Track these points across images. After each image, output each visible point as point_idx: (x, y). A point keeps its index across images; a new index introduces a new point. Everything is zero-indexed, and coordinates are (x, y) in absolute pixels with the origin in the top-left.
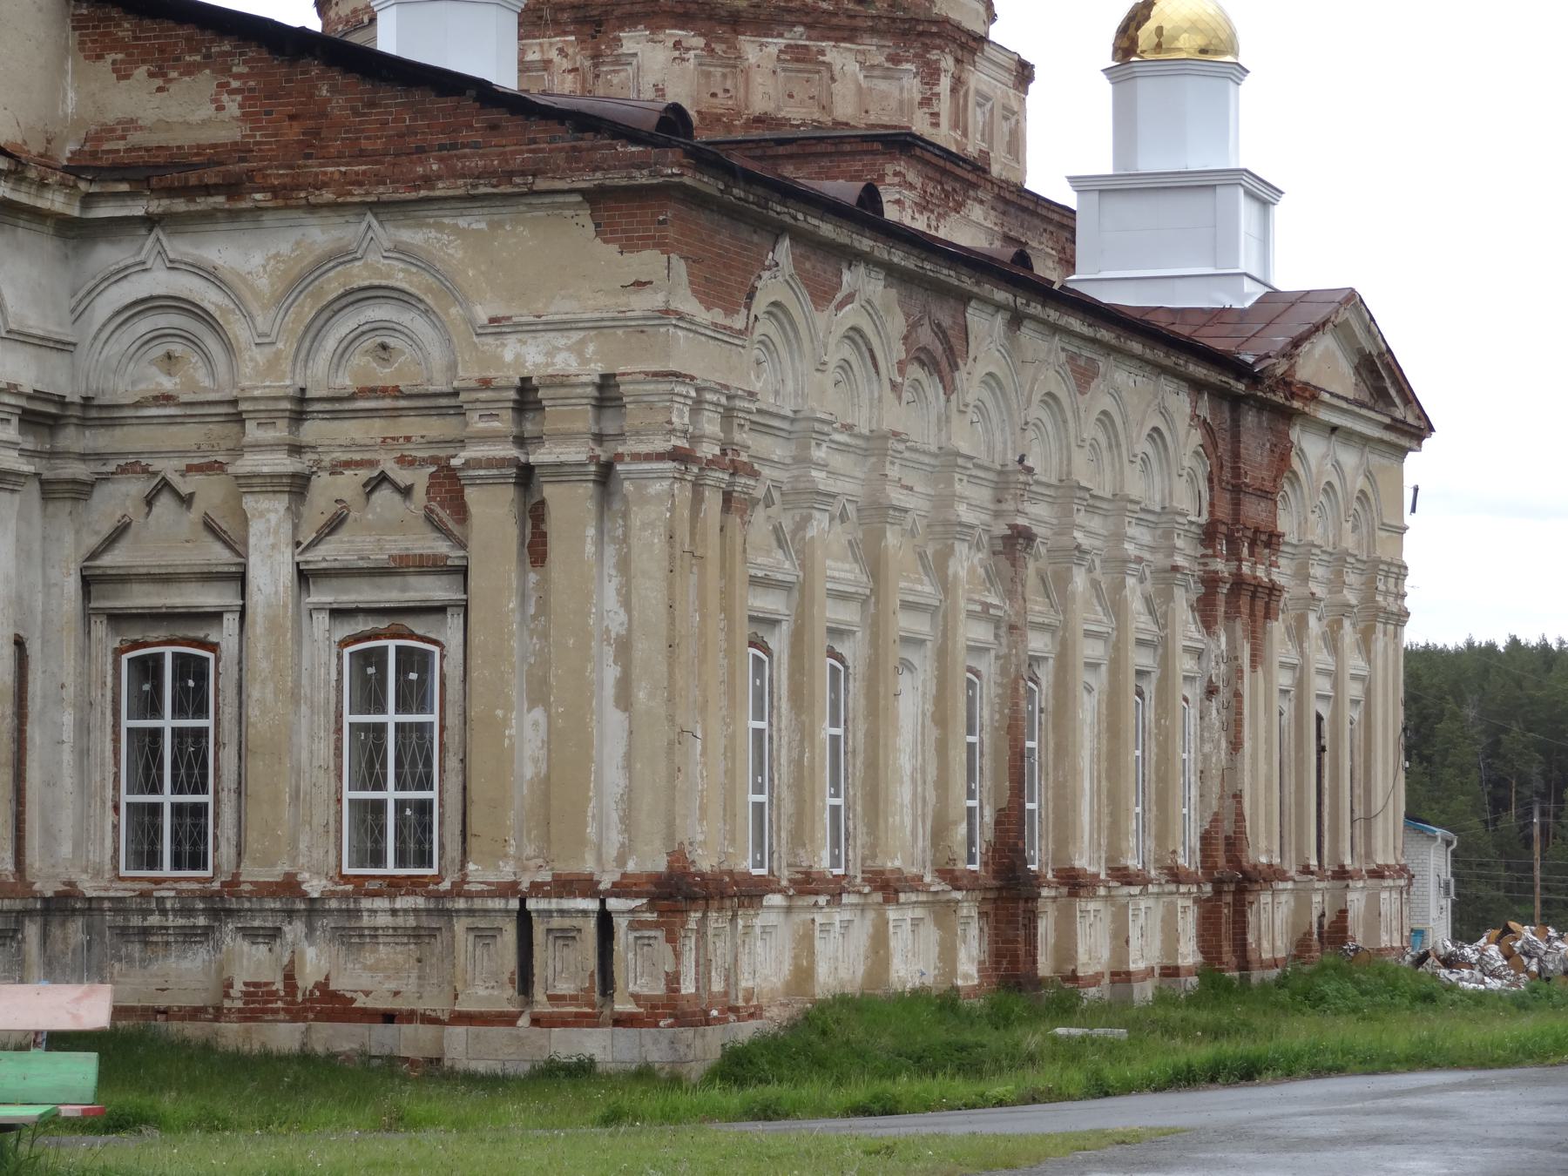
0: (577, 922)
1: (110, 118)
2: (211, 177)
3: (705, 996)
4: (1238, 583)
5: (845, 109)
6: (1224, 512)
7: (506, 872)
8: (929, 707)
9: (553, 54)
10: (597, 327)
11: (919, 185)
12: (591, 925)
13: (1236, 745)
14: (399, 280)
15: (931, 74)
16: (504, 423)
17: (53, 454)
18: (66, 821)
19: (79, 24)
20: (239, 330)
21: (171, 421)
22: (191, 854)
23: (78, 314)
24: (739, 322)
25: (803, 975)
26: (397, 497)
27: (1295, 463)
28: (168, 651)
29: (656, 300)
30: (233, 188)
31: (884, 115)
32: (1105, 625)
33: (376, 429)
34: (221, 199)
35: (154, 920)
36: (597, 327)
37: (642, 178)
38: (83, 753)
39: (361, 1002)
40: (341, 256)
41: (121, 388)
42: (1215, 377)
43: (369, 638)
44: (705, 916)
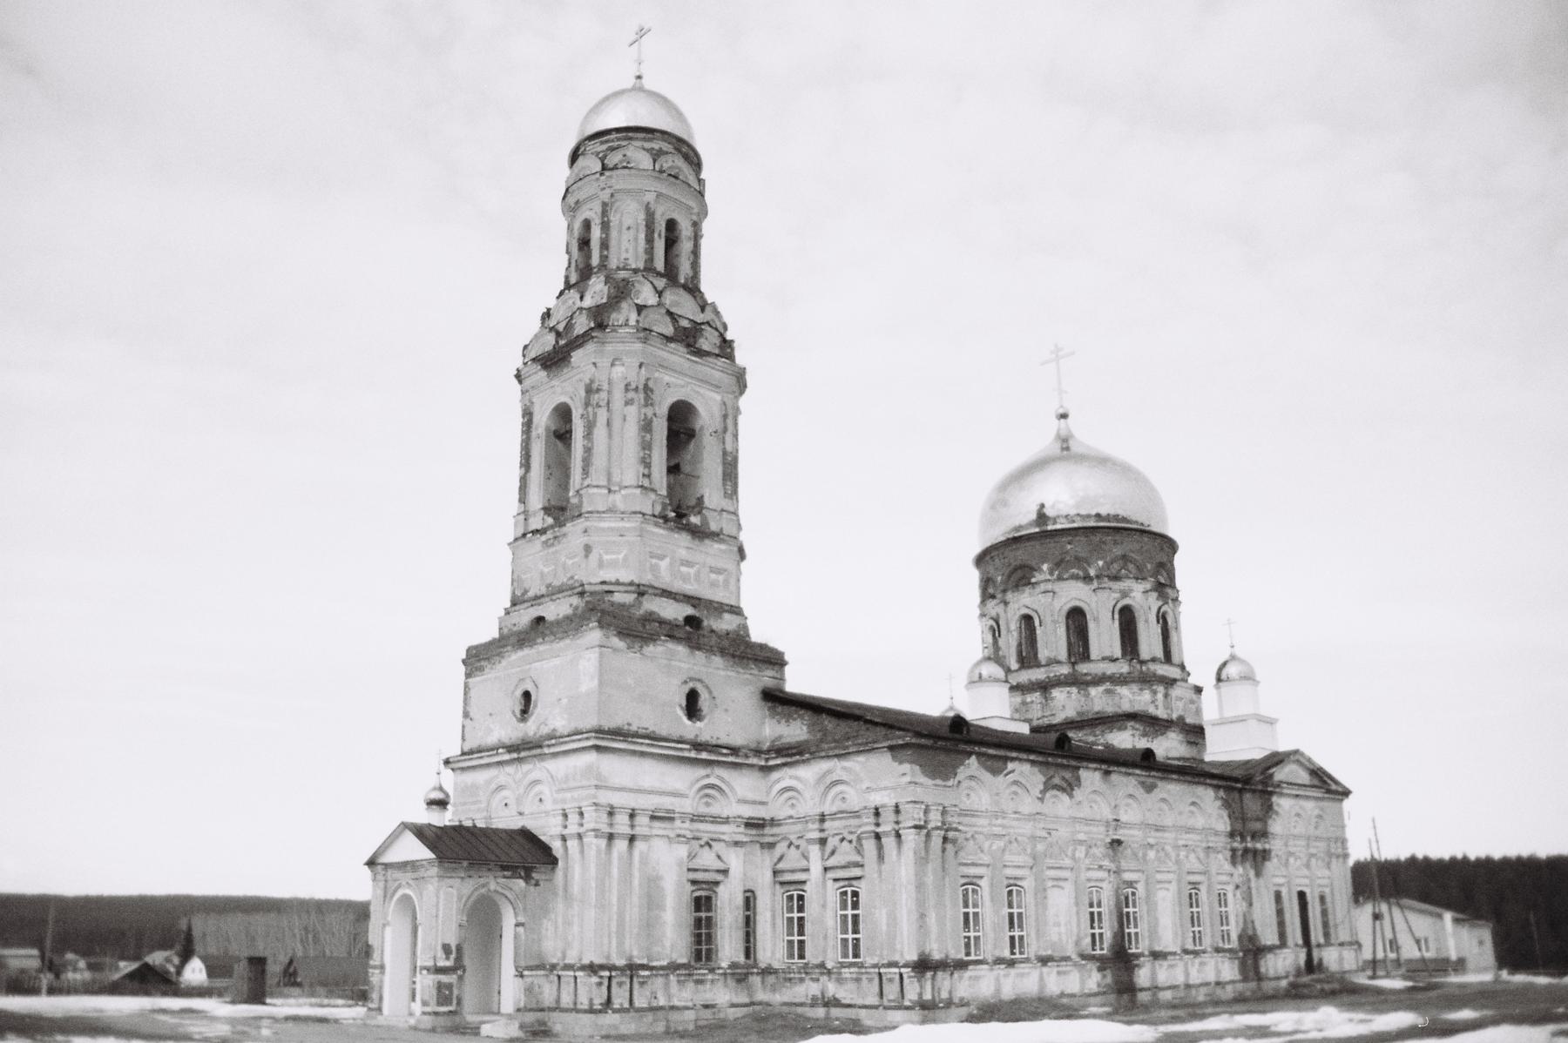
0: (894, 976)
1: (777, 735)
2: (794, 751)
3: (937, 999)
4: (1246, 851)
5: (1126, 707)
6: (1239, 826)
7: (875, 960)
8: (1073, 901)
9: (1034, 699)
10: (893, 788)
11: (1142, 728)
12: (898, 977)
13: (1251, 905)
14: (844, 778)
15: (1155, 693)
16: (872, 820)
17: (763, 835)
18: (769, 945)
19: (769, 709)
20: (807, 795)
21: (793, 823)
22: (801, 956)
23: (768, 793)
24: (950, 783)
25: (998, 991)
26: (848, 844)
27: (1276, 808)
28: (795, 893)
29: (908, 779)
30: (801, 753)
31: (1137, 708)
32: (1174, 868)
33: (844, 822)
34: (798, 757)
35: (792, 975)
36: (893, 788)
37: (901, 742)
38: (774, 925)
39: (844, 1001)
40: (829, 772)
41: (781, 813)
42: (1220, 783)
43: (843, 887)
44: (935, 973)
